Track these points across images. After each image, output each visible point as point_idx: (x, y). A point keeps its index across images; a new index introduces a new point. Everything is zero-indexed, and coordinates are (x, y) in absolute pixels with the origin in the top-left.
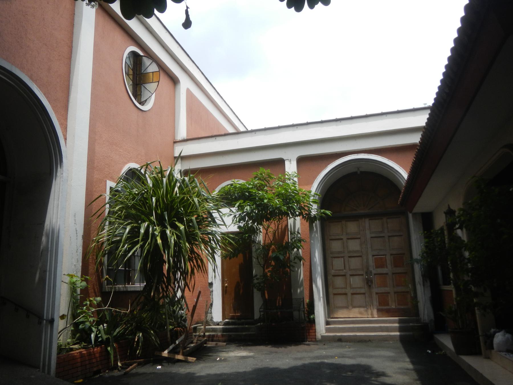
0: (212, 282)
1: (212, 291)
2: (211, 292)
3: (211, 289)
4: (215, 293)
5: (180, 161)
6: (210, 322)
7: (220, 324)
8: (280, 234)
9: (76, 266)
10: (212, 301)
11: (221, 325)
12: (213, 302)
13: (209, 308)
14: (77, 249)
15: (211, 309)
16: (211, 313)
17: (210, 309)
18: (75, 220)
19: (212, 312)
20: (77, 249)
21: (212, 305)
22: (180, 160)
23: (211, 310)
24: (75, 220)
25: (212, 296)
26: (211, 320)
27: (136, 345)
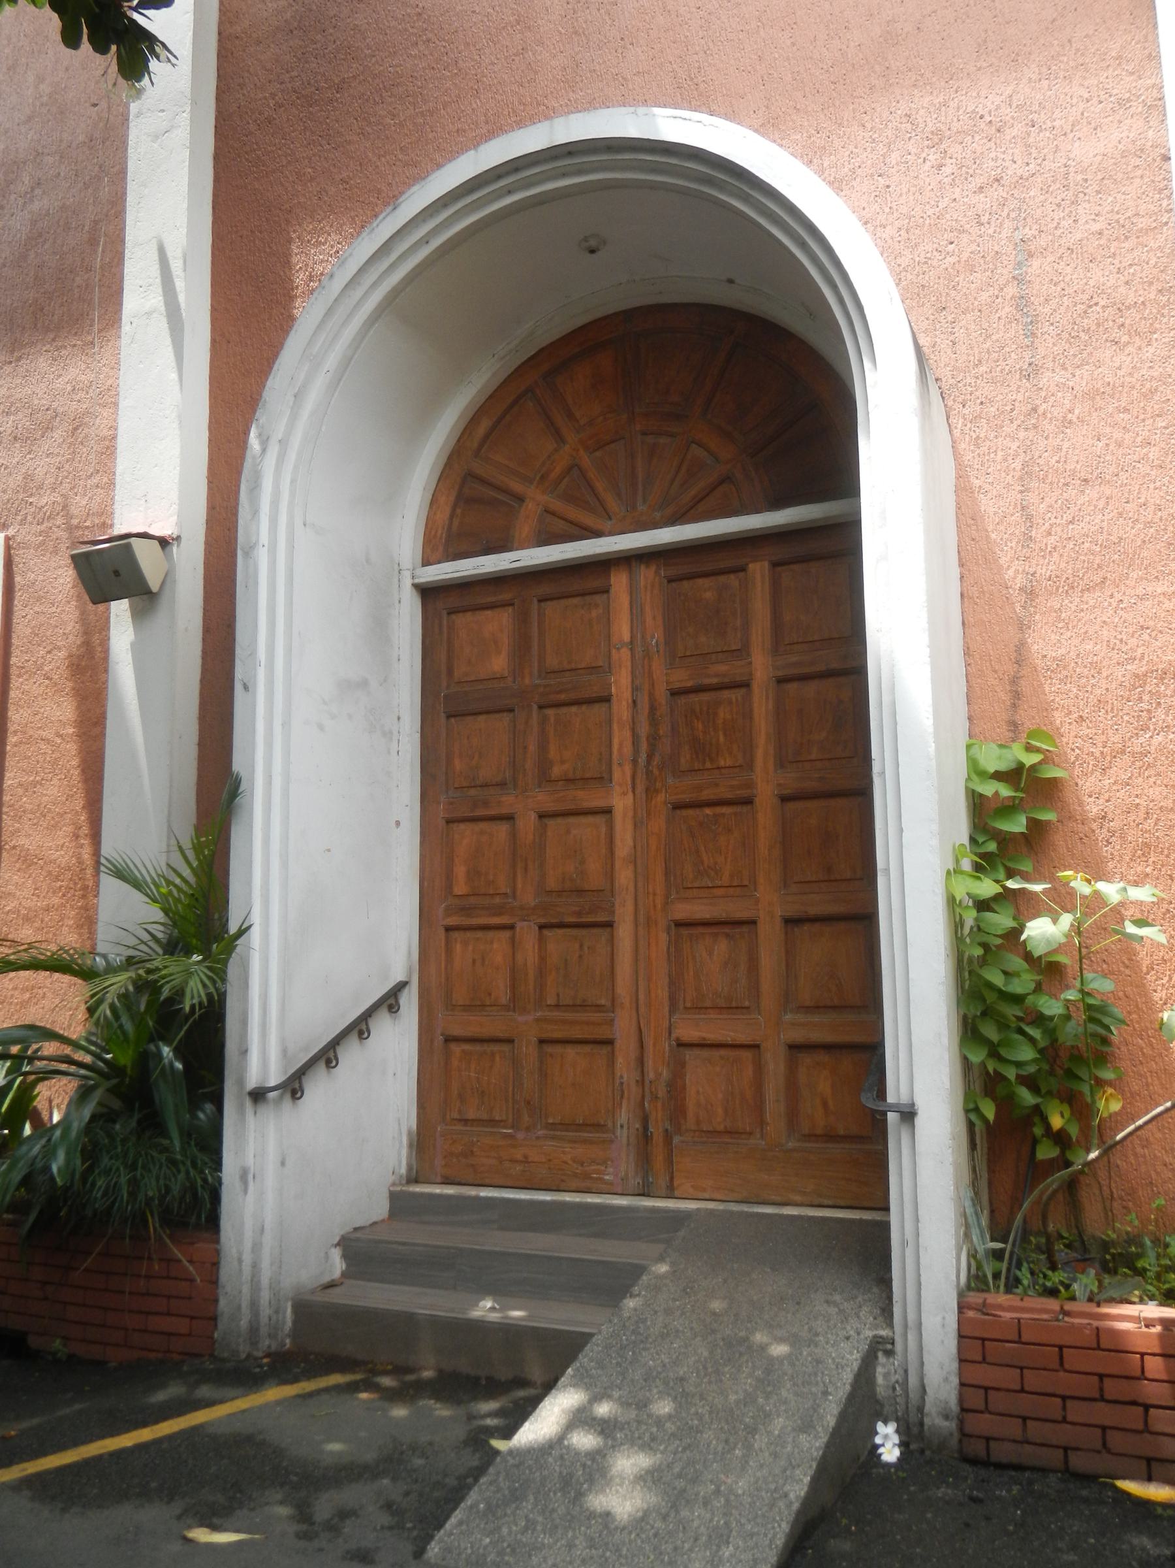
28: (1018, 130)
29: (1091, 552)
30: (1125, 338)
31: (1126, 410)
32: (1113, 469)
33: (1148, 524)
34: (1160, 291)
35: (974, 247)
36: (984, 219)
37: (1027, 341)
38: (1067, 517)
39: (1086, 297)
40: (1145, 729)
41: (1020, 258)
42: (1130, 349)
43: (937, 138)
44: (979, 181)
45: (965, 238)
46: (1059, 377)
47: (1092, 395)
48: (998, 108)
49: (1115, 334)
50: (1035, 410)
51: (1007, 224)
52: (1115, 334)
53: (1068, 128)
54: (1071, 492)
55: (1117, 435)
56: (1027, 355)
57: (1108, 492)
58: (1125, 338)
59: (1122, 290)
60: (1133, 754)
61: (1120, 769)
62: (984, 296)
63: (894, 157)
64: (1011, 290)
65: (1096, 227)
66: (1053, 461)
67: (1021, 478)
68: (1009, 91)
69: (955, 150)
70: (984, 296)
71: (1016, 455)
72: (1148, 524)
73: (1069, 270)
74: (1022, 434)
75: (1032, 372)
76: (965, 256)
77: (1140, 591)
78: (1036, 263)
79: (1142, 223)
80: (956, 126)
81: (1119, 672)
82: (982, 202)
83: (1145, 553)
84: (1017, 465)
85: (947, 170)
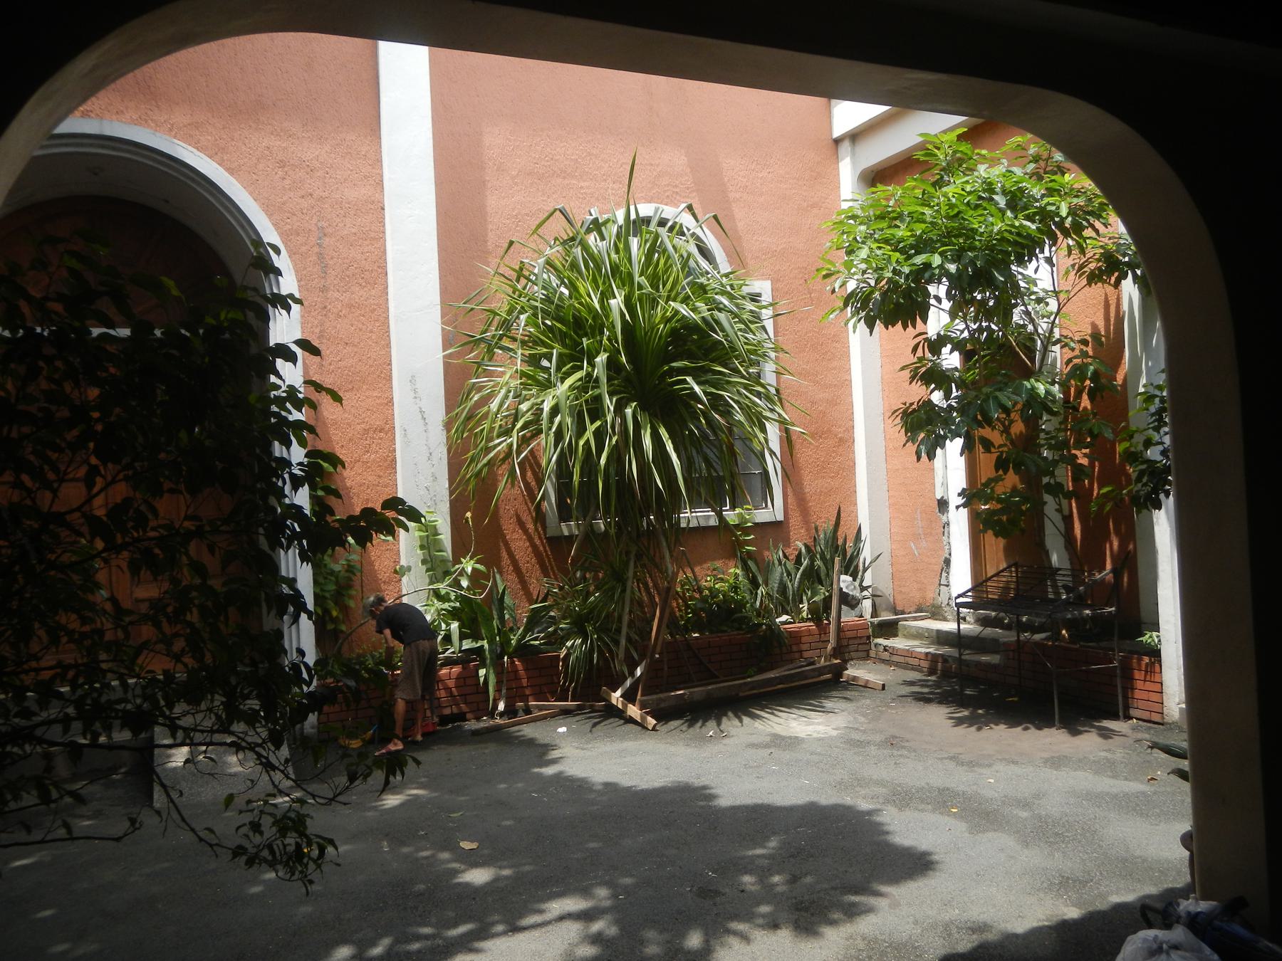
0: (943, 497)
1: (948, 524)
2: (944, 527)
3: (944, 518)
4: (954, 528)
5: (849, 149)
6: (945, 609)
7: (968, 618)
8: (1114, 334)
9: (430, 489)
10: (947, 551)
11: (969, 623)
12: (950, 555)
13: (942, 571)
14: (431, 454)
15: (948, 573)
16: (947, 586)
17: (944, 574)
18: (415, 392)
19: (951, 584)
20: (431, 454)
21: (947, 562)
22: (846, 147)
23: (947, 578)
24: (415, 392)
25: (949, 537)
26: (948, 604)
27: (562, 666)
28: (320, 173)
29: (348, 375)
30: (364, 284)
31: (363, 316)
32: (357, 340)
33: (371, 366)
34: (379, 267)
35: (299, 224)
36: (305, 211)
37: (323, 275)
38: (338, 358)
39: (348, 261)
40: (368, 452)
41: (320, 235)
42: (366, 289)
43: (282, 164)
44: (303, 193)
45: (295, 218)
46: (336, 295)
47: (350, 306)
48: (312, 160)
49: (361, 281)
50: (325, 307)
51: (315, 217)
52: (361, 281)
53: (342, 180)
54: (340, 347)
55: (360, 326)
56: (323, 281)
57: (356, 350)
58: (364, 284)
59: (364, 262)
60: (363, 462)
61: (358, 468)
62: (304, 249)
63: (261, 166)
64: (316, 249)
65: (353, 230)
66: (333, 332)
67: (319, 338)
68: (317, 153)
69: (290, 173)
70: (304, 249)
71: (317, 326)
72: (371, 366)
73: (341, 247)
74: (320, 317)
75: (324, 289)
76: (295, 227)
77: (367, 394)
78: (327, 240)
79: (373, 235)
80: (292, 162)
81: (359, 427)
82: (305, 204)
83: (369, 379)
84: (317, 330)
85: (287, 182)
